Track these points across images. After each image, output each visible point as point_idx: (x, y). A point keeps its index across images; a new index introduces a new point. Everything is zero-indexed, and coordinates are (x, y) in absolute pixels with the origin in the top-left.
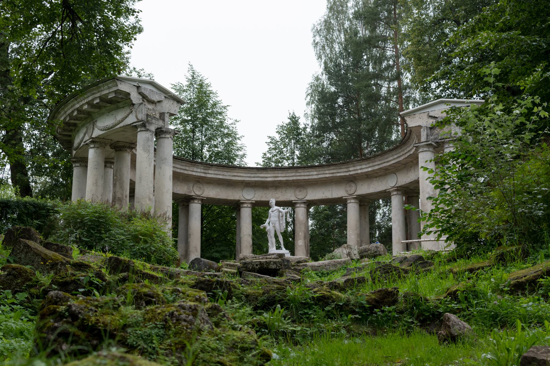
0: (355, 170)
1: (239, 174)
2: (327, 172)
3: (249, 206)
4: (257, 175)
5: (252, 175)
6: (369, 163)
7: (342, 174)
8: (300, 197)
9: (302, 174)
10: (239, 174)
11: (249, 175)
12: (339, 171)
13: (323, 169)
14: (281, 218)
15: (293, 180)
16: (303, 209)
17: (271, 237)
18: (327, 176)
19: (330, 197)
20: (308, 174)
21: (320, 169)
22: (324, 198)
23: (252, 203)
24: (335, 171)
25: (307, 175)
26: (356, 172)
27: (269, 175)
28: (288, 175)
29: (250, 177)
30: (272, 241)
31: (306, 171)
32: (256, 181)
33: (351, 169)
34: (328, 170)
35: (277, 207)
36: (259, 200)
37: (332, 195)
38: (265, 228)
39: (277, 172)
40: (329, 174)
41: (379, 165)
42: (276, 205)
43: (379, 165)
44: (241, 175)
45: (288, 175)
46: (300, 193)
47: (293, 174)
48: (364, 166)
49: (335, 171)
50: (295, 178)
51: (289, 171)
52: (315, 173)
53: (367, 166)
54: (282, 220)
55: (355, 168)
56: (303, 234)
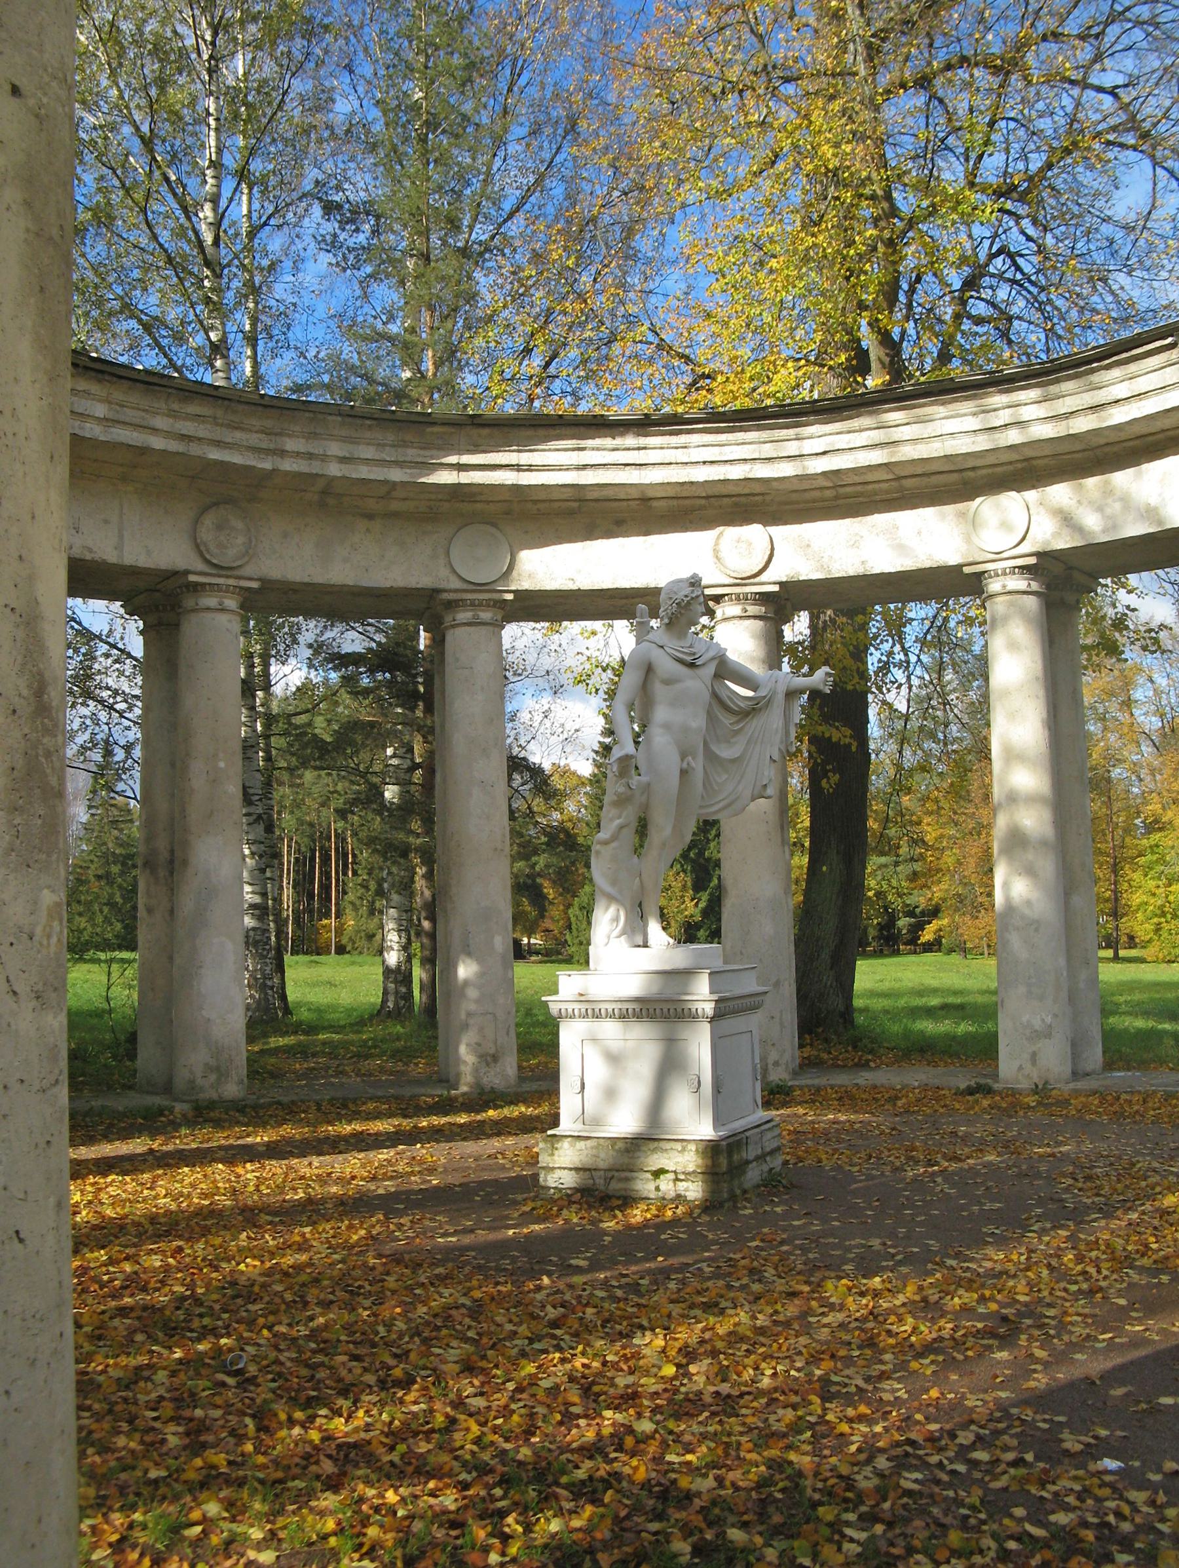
0: (310, 456)
2: (160, 422)
6: (405, 444)
7: (236, 459)
18: (158, 443)
24: (202, 431)
26: (315, 467)
33: (291, 445)
34: (173, 414)
37: (119, 547)
40: (168, 434)
41: (461, 468)
43: (461, 468)
48: (368, 452)
49: (202, 431)
52: (100, 410)
55: (315, 447)
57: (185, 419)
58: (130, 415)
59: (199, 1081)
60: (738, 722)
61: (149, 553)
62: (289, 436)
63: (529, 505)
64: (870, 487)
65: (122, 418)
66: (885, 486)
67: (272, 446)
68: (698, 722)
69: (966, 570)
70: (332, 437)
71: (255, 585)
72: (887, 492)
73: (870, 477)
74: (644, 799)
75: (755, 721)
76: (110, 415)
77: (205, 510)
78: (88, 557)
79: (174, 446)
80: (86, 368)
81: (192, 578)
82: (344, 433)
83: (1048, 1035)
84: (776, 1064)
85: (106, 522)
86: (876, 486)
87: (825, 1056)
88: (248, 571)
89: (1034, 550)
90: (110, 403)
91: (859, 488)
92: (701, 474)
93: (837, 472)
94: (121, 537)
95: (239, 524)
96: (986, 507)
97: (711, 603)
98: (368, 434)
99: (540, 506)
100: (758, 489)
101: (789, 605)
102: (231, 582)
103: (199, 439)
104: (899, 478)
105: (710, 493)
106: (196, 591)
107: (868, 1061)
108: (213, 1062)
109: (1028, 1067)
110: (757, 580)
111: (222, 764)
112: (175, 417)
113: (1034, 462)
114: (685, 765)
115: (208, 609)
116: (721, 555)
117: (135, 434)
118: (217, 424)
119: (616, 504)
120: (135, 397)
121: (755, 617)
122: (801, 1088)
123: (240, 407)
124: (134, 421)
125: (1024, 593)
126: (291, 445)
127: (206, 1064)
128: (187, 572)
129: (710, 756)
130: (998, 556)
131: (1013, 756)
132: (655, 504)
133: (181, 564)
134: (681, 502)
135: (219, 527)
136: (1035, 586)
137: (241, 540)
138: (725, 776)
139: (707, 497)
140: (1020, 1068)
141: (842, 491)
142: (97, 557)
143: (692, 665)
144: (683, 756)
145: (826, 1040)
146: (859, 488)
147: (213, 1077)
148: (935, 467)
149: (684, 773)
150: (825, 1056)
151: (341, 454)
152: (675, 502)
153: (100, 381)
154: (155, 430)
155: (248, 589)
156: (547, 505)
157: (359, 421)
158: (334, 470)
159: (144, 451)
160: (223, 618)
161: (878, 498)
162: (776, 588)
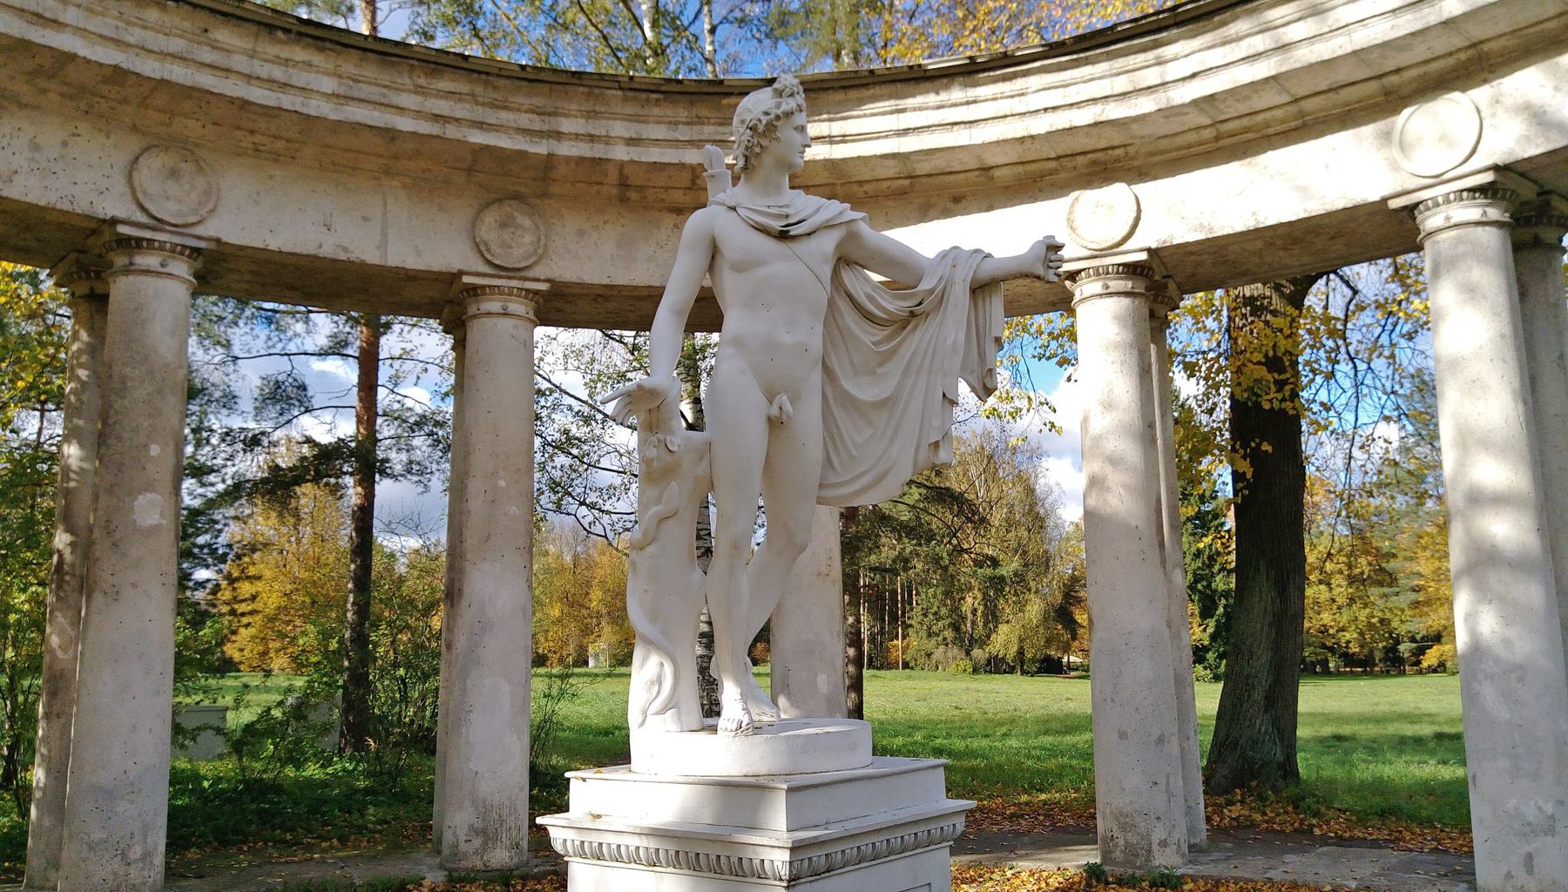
0: (592, 138)
2: (408, 100)
6: (699, 121)
8: (166, 210)
9: (239, 62)
12: (492, 116)
13: (385, 77)
18: (405, 124)
19: (369, 254)
22: (327, 251)
25: (271, 82)
26: (597, 151)
28: (134, 35)
31: (272, 49)
33: (567, 125)
37: (382, 246)
40: (418, 114)
46: (173, 188)
48: (660, 132)
50: (178, 73)
52: (328, 85)
53: (683, 133)
55: (597, 128)
58: (366, 91)
59: (463, 847)
60: (889, 338)
61: (419, 254)
62: (565, 115)
63: (855, 188)
64: (1260, 118)
65: (356, 94)
66: (1278, 113)
67: (545, 128)
68: (811, 334)
69: (1394, 204)
70: (614, 116)
71: (543, 287)
72: (1283, 121)
73: (1259, 103)
74: (702, 469)
75: (918, 334)
76: (342, 91)
77: (486, 206)
78: (343, 257)
79: (425, 128)
80: (300, 34)
81: (466, 279)
82: (629, 110)
83: (1551, 831)
84: (1163, 844)
85: (365, 219)
86: (1268, 115)
87: (1258, 817)
88: (538, 272)
89: (1489, 162)
90: (340, 77)
91: (1245, 122)
92: (1041, 125)
93: (1211, 98)
94: (384, 235)
95: (527, 223)
96: (1417, 120)
97: (1067, 283)
98: (656, 111)
99: (867, 187)
100: (1116, 138)
101: (1172, 285)
102: (514, 283)
103: (457, 120)
104: (1296, 101)
105: (1061, 152)
106: (476, 295)
107: (1312, 826)
108: (479, 824)
109: (1521, 877)
110: (1122, 248)
111: (502, 483)
113: (1485, 47)
114: (775, 411)
115: (489, 314)
116: (1076, 225)
117: (376, 114)
118: (477, 103)
119: (952, 178)
120: (371, 71)
121: (1118, 294)
122: (1194, 879)
123: (502, 82)
124: (377, 99)
125: (1478, 223)
126: (567, 125)
127: (471, 827)
128: (461, 273)
129: (835, 397)
130: (1439, 179)
131: (1468, 440)
132: (997, 173)
133: (455, 265)
134: (1028, 168)
135: (503, 225)
136: (1494, 213)
137: (528, 238)
138: (869, 432)
139: (1058, 158)
140: (1509, 876)
141: (1224, 128)
142: (353, 257)
143: (783, 236)
144: (771, 397)
145: (1262, 798)
146: (1245, 122)
147: (477, 842)
148: (1343, 75)
149: (775, 424)
150: (1258, 817)
151: (627, 135)
152: (1020, 169)
153: (322, 50)
155: (536, 292)
156: (874, 185)
157: (644, 96)
158: (621, 153)
159: (391, 134)
160: (507, 323)
161: (1271, 131)
162: (1143, 256)
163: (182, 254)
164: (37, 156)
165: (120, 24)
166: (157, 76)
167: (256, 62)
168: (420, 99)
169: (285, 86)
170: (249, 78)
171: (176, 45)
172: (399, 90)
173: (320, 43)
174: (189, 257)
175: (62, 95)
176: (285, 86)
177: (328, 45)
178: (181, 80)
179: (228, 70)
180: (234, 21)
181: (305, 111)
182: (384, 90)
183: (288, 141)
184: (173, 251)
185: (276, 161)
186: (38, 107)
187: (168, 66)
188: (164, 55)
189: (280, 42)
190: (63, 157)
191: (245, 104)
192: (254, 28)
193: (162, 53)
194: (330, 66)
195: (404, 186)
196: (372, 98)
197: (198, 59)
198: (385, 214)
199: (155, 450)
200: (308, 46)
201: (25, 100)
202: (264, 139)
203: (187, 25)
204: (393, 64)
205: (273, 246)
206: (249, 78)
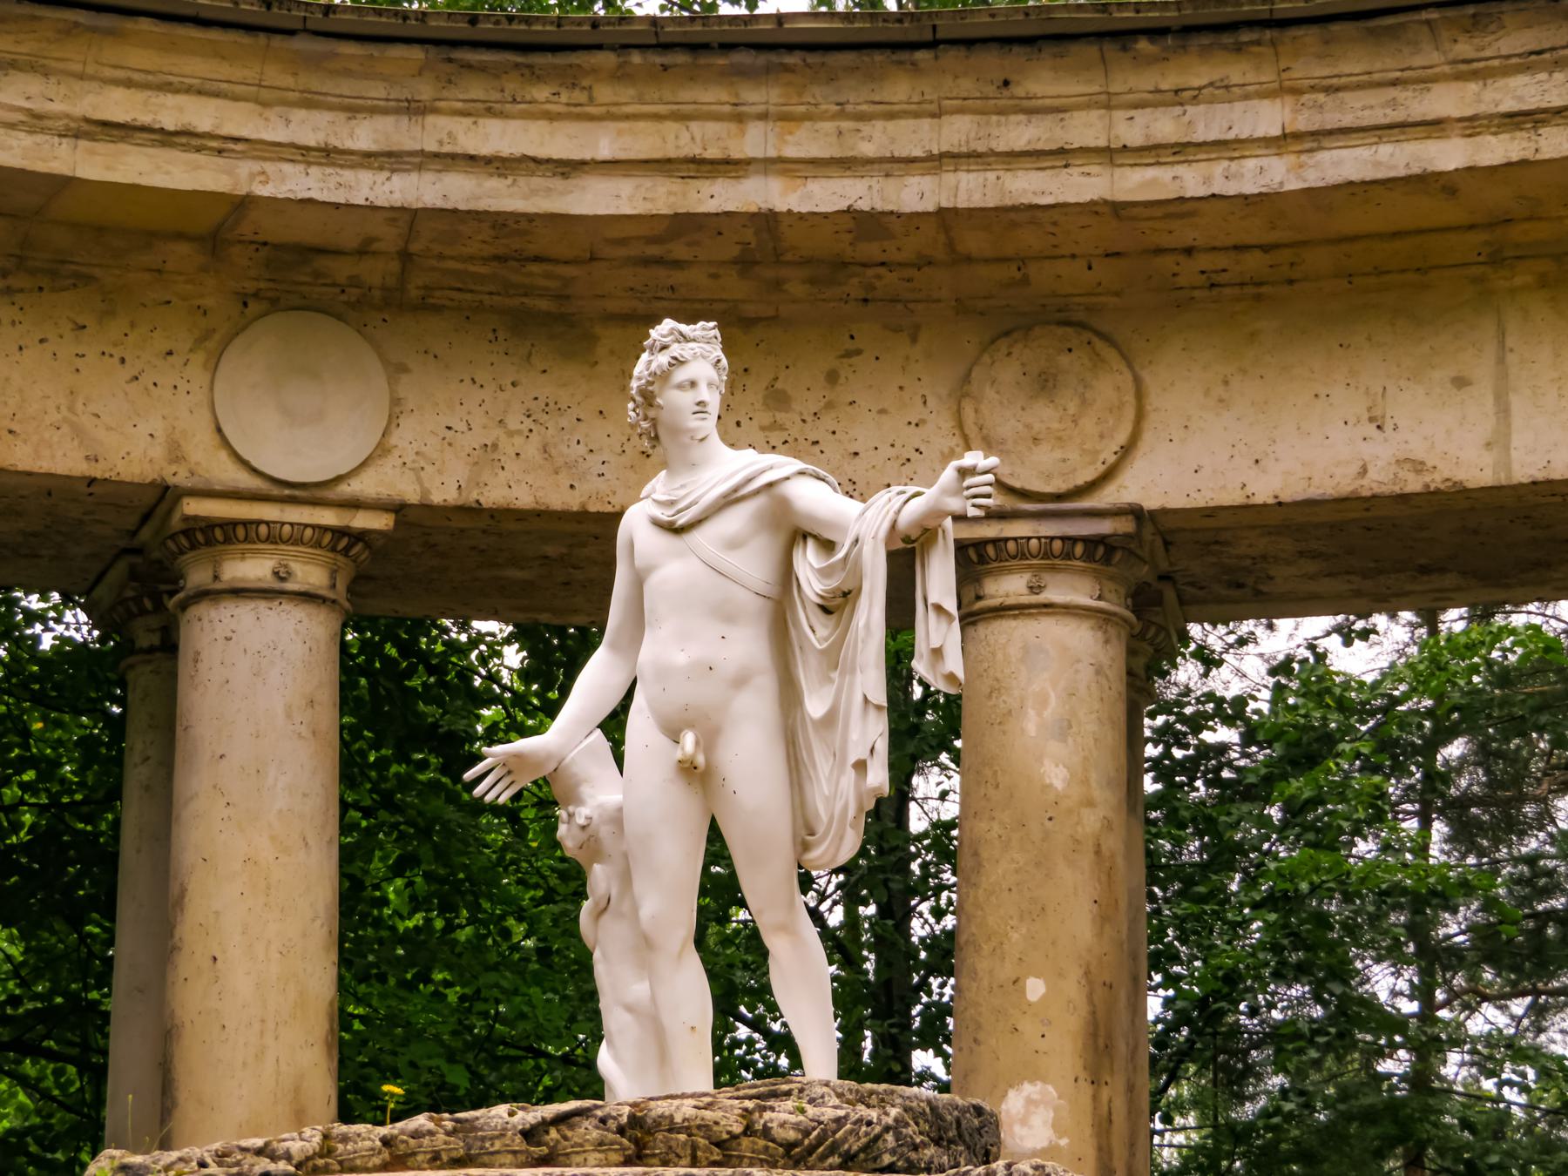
1: (171, 112)
2: (1446, 101)
3: (310, 574)
4: (433, 133)
5: (364, 135)
9: (1086, 129)
10: (171, 112)
11: (309, 128)
13: (1386, 63)
14: (814, 632)
15: (945, 217)
16: (1081, 639)
17: (645, 946)
18: (1448, 155)
19: (1474, 466)
20: (1164, 126)
21: (1352, 65)
22: (1382, 478)
23: (342, 540)
25: (1154, 152)
27: (605, 143)
28: (873, 140)
29: (328, 155)
30: (653, 1023)
31: (1144, 81)
32: (410, 218)
35: (729, 464)
36: (444, 493)
37: (1499, 441)
38: (544, 798)
39: (712, 95)
40: (1472, 125)
42: (733, 431)
44: (203, 115)
45: (873, 140)
46: (1044, 415)
47: (957, 132)
50: (970, 189)
51: (899, 90)
52: (1269, 118)
54: (833, 658)
56: (1073, 988)
57: (1507, 71)
65: (1332, 119)
76: (1303, 122)
78: (1414, 484)
79: (1497, 150)
85: (1461, 382)
90: (1296, 92)
112: (1475, 75)
117: (1385, 150)
142: (1436, 480)
153: (1239, 49)
154: (1435, 127)
163: (1068, 556)
164: (781, 417)
165: (846, 125)
166: (929, 206)
167: (1119, 115)
168: (1473, 87)
169: (1181, 151)
170: (1110, 155)
171: (957, 132)
172: (1426, 81)
173: (1227, 39)
174: (1088, 556)
175: (812, 281)
176: (1181, 151)
177: (1245, 36)
178: (977, 201)
179: (1061, 152)
180: (1049, 49)
181: (1231, 189)
182: (1393, 92)
183: (1266, 248)
184: (1047, 554)
185: (1258, 298)
186: (773, 320)
187: (949, 178)
188: (937, 162)
189: (1151, 61)
190: (830, 406)
191: (1118, 210)
192: (1091, 51)
193: (930, 158)
194: (1268, 76)
195: (1543, 282)
196: (1369, 118)
197: (1001, 147)
198: (1501, 361)
199: (1035, 988)
200: (1205, 52)
201: (751, 310)
202: (1221, 261)
203: (967, 86)
204: (1393, 33)
205: (1263, 496)
206: (1110, 155)
